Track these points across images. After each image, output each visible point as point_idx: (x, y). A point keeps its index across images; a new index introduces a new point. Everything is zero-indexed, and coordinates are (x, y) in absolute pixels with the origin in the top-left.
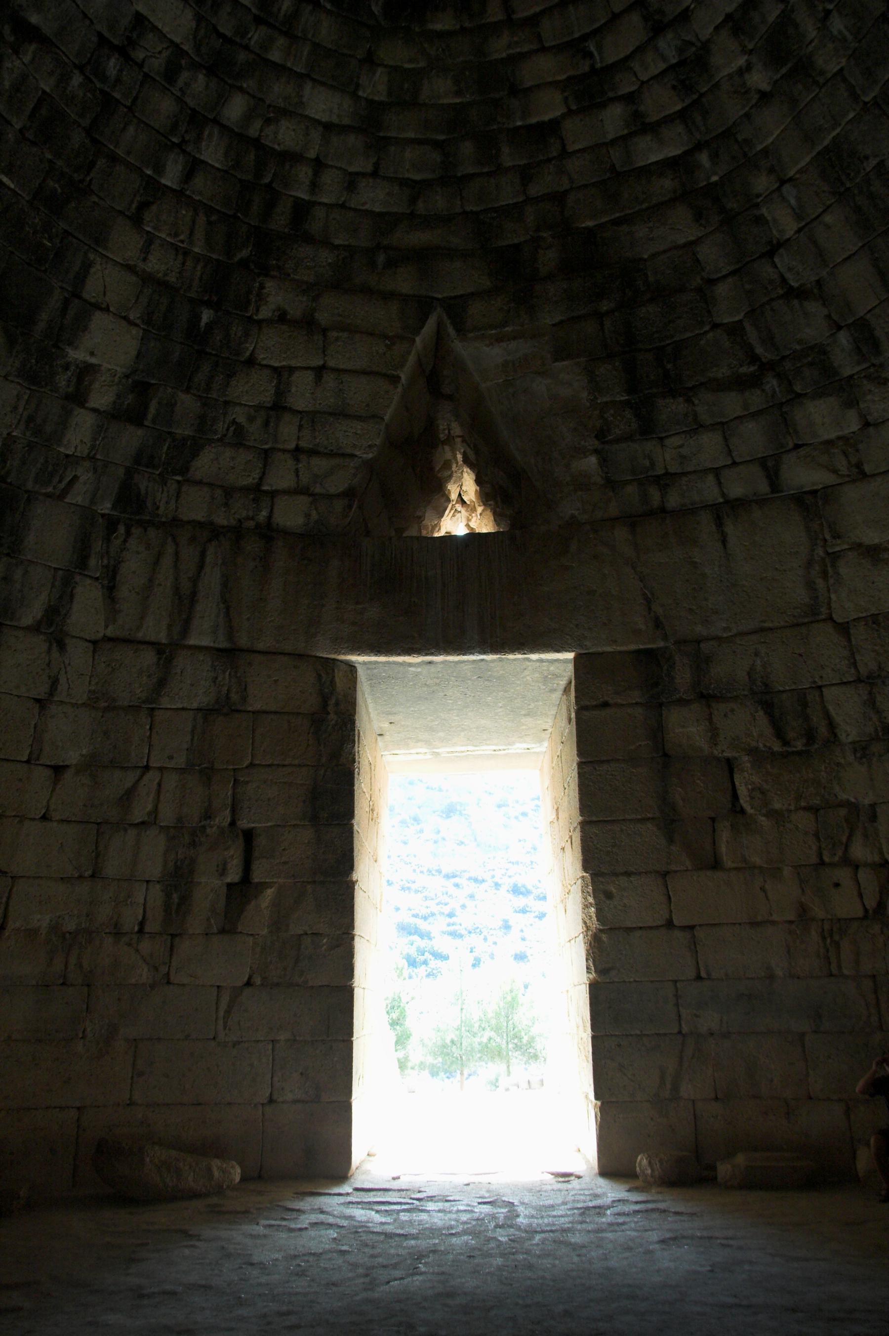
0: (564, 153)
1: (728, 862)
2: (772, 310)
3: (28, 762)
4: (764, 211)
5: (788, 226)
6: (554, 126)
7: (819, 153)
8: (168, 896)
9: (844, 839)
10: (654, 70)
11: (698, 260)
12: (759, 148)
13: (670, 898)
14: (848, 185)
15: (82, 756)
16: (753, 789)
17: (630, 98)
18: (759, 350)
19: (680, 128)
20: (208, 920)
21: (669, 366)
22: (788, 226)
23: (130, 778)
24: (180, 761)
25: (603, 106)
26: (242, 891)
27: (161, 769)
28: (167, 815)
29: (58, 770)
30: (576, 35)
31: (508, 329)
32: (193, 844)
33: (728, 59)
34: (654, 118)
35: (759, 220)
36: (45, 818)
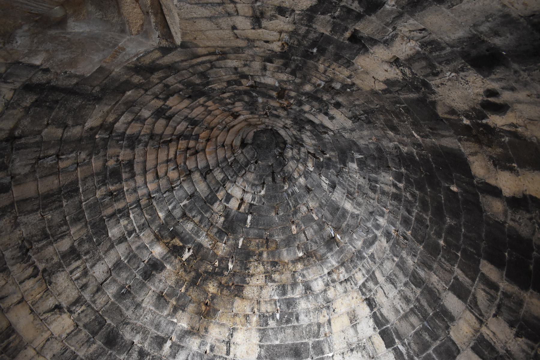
0: (157, 97)
2: (37, 151)
4: (74, 155)
5: (62, 165)
6: (166, 99)
7: (78, 181)
10: (144, 130)
11: (77, 125)
12: (94, 157)
14: (63, 193)
17: (146, 119)
18: (23, 141)
19: (122, 131)
21: (48, 104)
22: (62, 165)
25: (152, 114)
30: (176, 116)
31: (135, 59)
33: (124, 154)
34: (132, 123)
35: (72, 152)
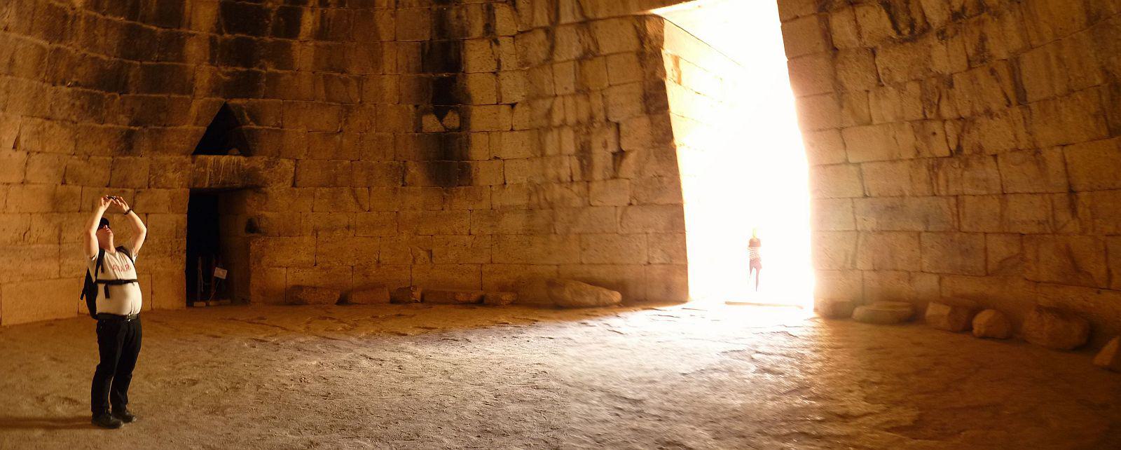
1: (875, 122)
3: (497, 104)
8: (581, 162)
9: (936, 101)
13: (845, 144)
15: (524, 96)
16: (885, 69)
20: (603, 171)
23: (548, 103)
24: (572, 89)
26: (620, 155)
27: (563, 96)
28: (571, 119)
29: (513, 106)
32: (588, 133)
36: (512, 130)
